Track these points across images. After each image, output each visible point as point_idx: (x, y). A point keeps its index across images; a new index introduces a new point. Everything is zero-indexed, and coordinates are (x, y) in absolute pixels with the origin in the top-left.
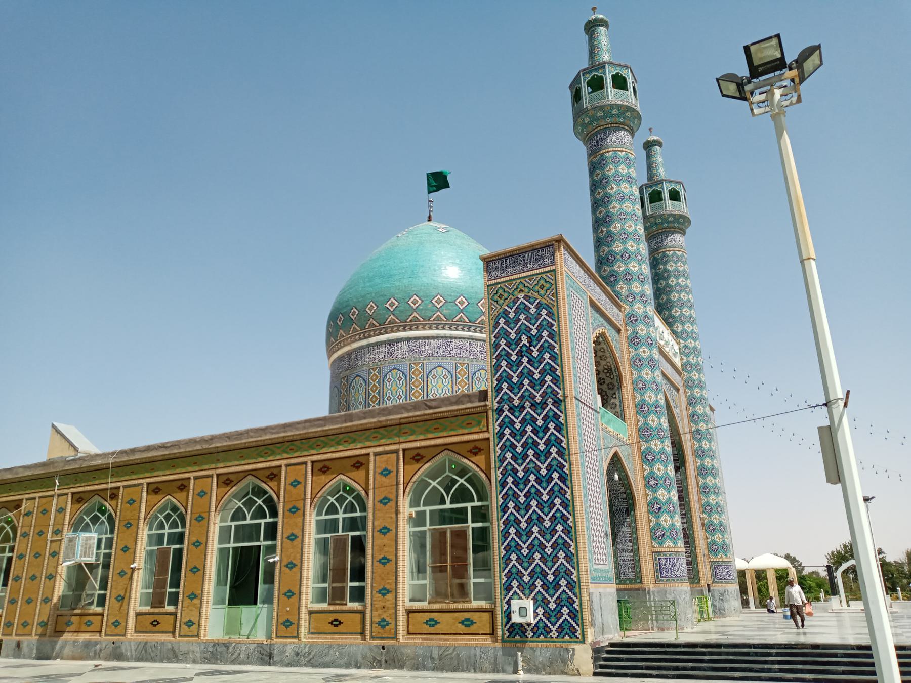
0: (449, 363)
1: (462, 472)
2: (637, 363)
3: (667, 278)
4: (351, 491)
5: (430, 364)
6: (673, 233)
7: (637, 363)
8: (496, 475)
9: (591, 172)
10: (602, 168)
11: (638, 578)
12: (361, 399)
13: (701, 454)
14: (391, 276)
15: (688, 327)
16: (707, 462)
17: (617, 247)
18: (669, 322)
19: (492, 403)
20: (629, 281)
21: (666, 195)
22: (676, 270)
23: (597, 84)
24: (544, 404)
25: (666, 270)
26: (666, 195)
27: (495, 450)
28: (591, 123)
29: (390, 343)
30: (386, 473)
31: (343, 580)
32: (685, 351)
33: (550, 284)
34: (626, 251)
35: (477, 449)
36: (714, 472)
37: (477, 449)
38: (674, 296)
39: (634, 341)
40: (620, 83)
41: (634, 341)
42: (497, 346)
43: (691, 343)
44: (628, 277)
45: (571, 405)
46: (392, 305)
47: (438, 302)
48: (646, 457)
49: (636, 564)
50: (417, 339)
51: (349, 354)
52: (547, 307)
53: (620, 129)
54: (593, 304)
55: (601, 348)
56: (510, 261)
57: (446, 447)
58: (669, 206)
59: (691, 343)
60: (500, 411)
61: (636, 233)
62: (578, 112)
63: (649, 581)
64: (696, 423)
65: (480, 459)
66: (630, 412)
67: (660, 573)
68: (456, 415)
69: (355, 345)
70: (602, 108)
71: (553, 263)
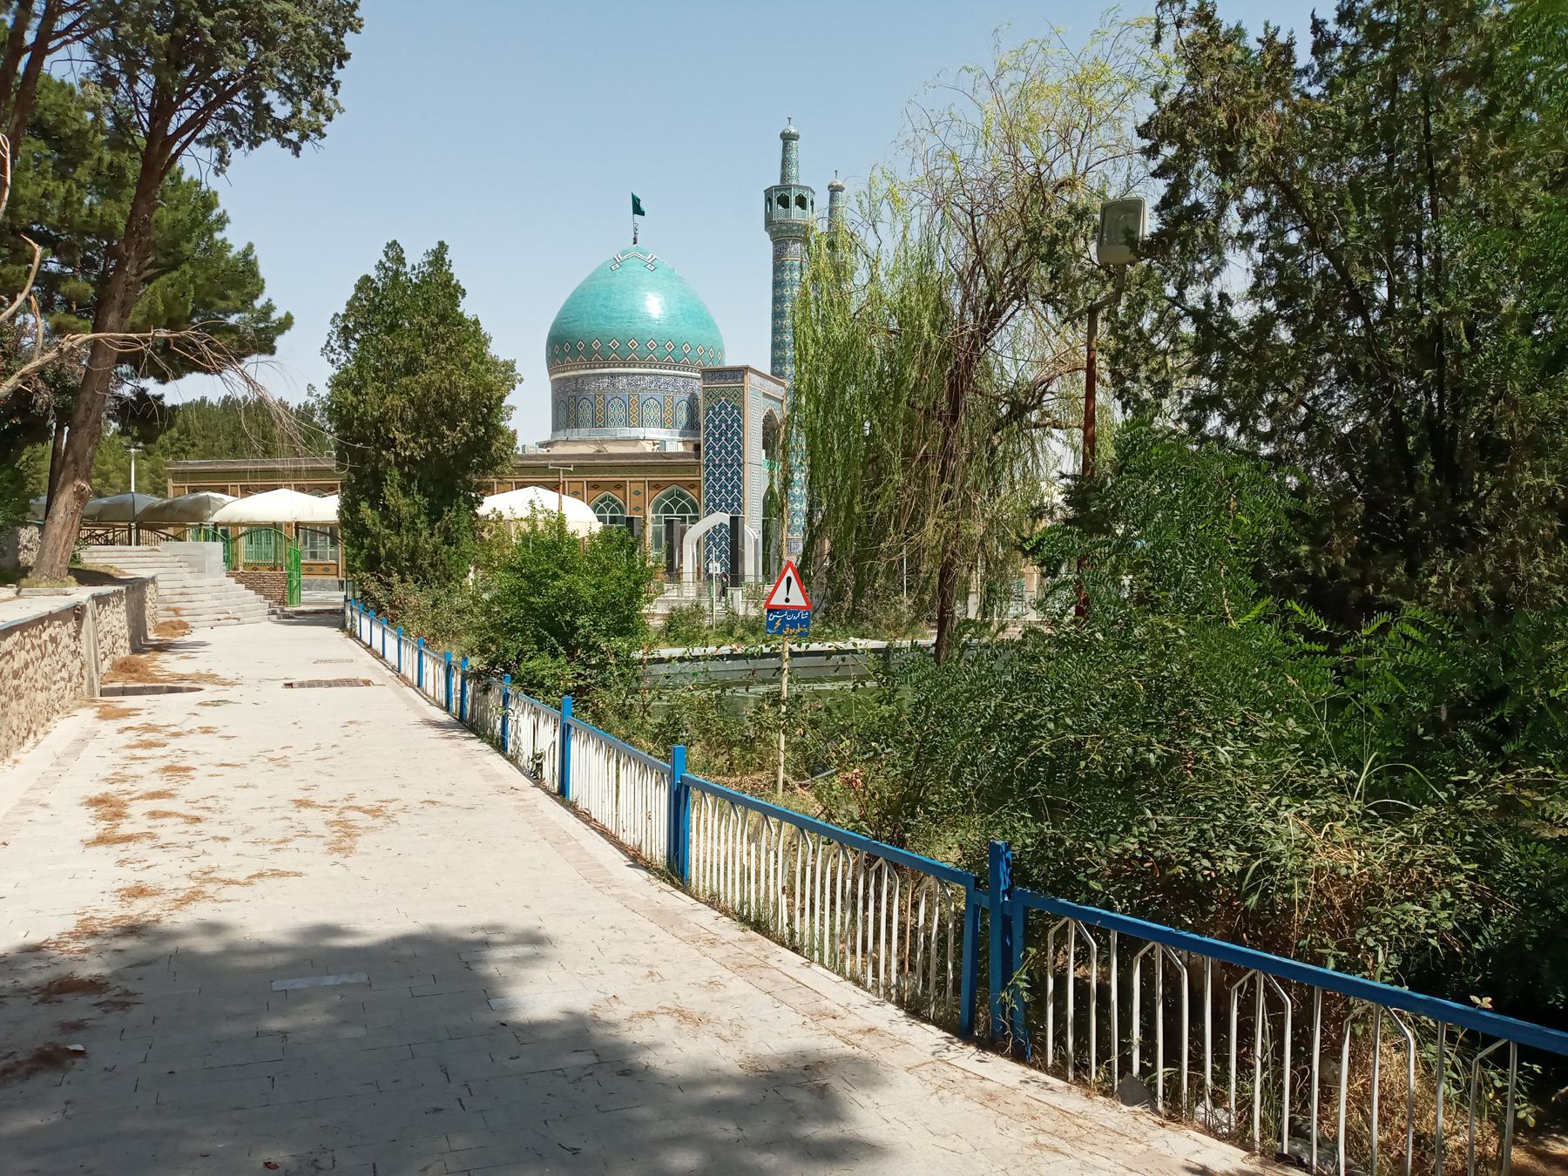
0: (659, 396)
4: (614, 501)
5: (645, 395)
8: (704, 501)
12: (589, 416)
14: (612, 318)
27: (704, 487)
29: (613, 375)
30: (637, 493)
33: (740, 394)
35: (693, 485)
37: (693, 485)
40: (801, 202)
51: (576, 378)
57: (675, 482)
62: (769, 223)
65: (695, 491)
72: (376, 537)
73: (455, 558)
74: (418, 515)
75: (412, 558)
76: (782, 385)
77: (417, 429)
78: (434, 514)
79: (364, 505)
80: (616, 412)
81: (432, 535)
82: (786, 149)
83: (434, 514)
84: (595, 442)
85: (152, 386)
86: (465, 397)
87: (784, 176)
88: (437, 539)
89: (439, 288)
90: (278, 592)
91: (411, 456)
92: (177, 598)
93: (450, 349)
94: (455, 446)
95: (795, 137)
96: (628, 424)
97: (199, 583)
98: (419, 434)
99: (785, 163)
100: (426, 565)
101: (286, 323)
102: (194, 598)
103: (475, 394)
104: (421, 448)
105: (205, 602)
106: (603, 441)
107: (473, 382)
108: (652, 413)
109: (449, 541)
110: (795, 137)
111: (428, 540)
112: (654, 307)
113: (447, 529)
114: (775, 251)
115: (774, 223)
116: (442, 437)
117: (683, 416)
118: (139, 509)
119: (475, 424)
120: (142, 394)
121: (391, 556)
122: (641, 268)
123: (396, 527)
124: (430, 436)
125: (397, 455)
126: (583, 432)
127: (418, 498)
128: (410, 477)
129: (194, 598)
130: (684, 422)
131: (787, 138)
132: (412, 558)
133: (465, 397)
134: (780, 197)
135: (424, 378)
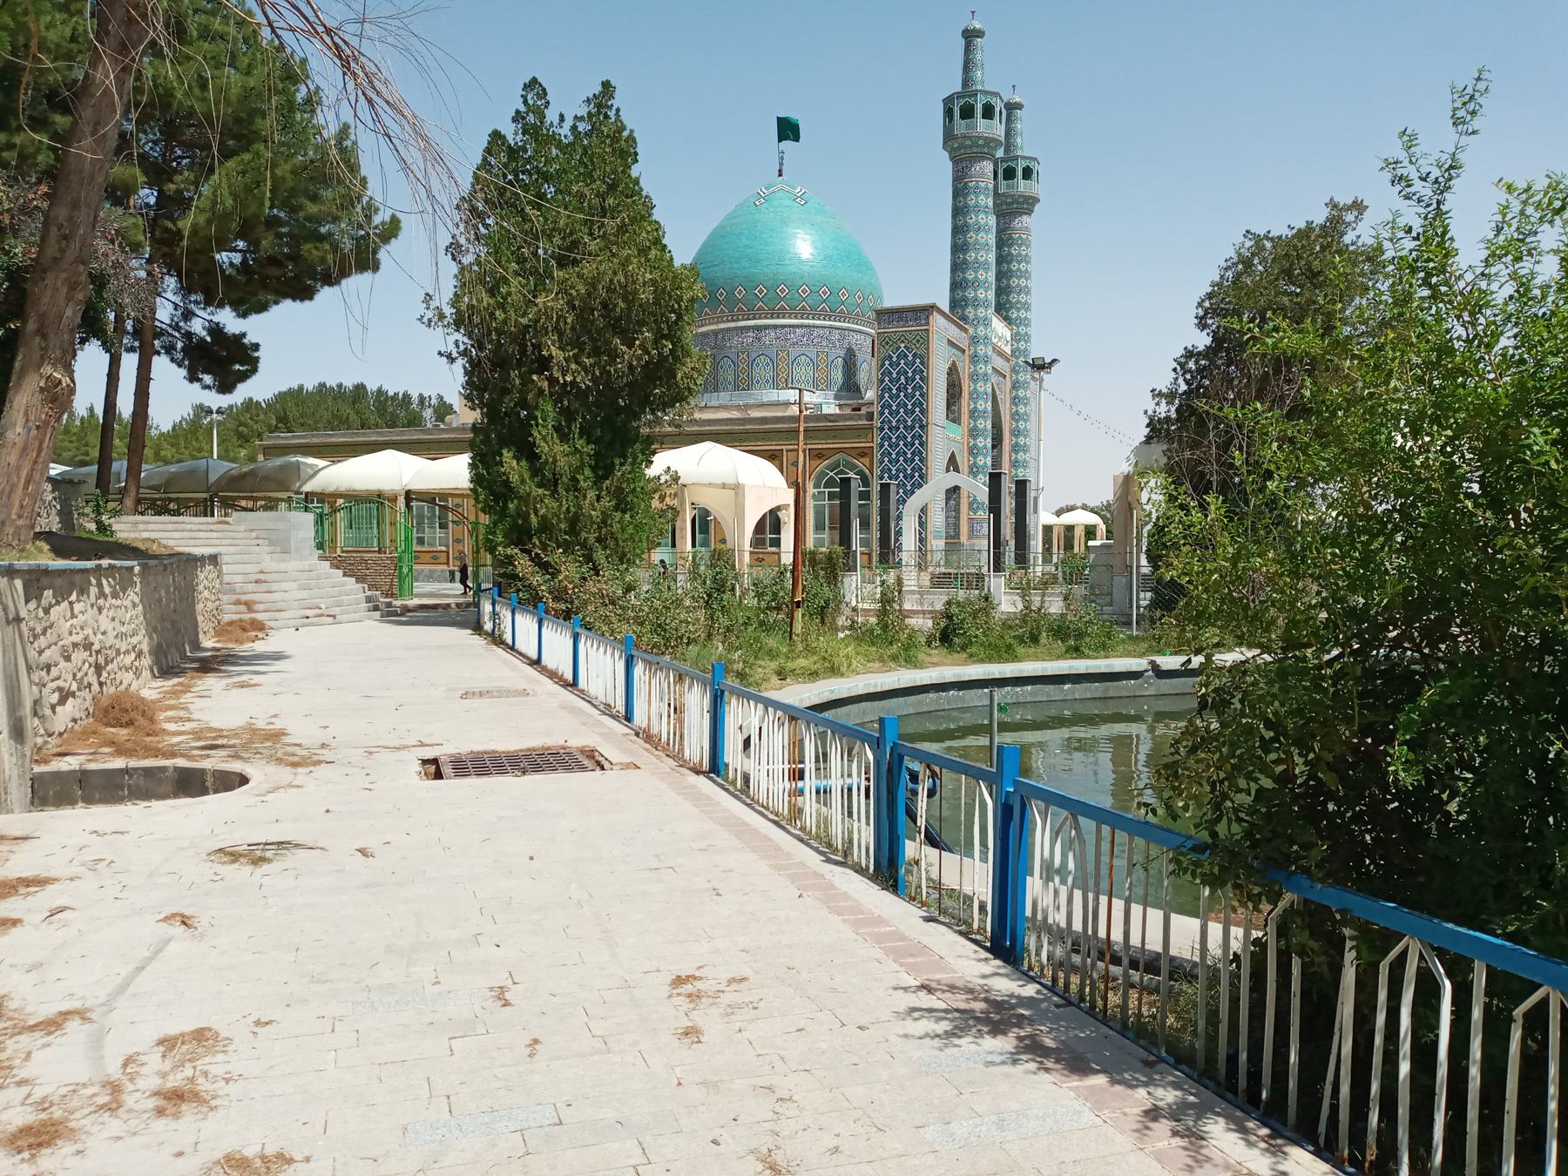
1: (853, 467)
2: (974, 377)
3: (1009, 263)
5: (794, 352)
6: (1021, 214)
7: (974, 377)
8: (877, 472)
9: (954, 216)
10: (965, 196)
11: (957, 535)
12: (730, 378)
13: (1016, 433)
15: (1022, 314)
16: (1021, 440)
17: (970, 275)
18: (1007, 320)
19: (877, 423)
20: (976, 307)
21: (1020, 173)
22: (1019, 255)
23: (968, 113)
24: (913, 427)
25: (1009, 254)
26: (1020, 173)
27: (877, 456)
28: (959, 148)
29: (758, 328)
31: (763, 532)
32: (1016, 337)
33: (924, 339)
34: (976, 280)
35: (863, 453)
36: (1025, 449)
37: (863, 453)
38: (1013, 298)
39: (975, 359)
40: (988, 112)
41: (975, 359)
42: (882, 381)
43: (1022, 329)
44: (976, 303)
45: (932, 430)
46: (761, 291)
47: (804, 291)
48: (973, 451)
49: (957, 526)
50: (783, 326)
51: (715, 333)
52: (921, 357)
53: (984, 159)
54: (950, 343)
55: (953, 371)
56: (896, 316)
57: (841, 450)
58: (1022, 186)
59: (1022, 329)
60: (882, 429)
61: (986, 262)
62: (949, 136)
63: (964, 538)
64: (1016, 405)
65: (866, 460)
66: (965, 417)
67: (972, 533)
68: (850, 428)
69: (722, 326)
70: (970, 138)
71: (927, 324)
72: (525, 499)
73: (630, 530)
74: (580, 469)
75: (573, 529)
76: (966, 331)
77: (580, 346)
78: (602, 470)
79: (507, 455)
80: (762, 371)
81: (599, 498)
82: (968, 49)
83: (602, 470)
84: (738, 407)
85: (228, 319)
86: (646, 295)
87: (966, 82)
88: (607, 503)
89: (605, 148)
90: (384, 581)
91: (574, 383)
92: (251, 587)
93: (622, 229)
94: (631, 367)
95: (979, 34)
96: (776, 386)
97: (283, 566)
98: (582, 351)
99: (968, 66)
100: (592, 538)
101: (391, 230)
102: (274, 587)
103: (659, 292)
104: (585, 369)
105: (289, 592)
106: (747, 407)
107: (656, 275)
108: (803, 373)
109: (622, 505)
110: (979, 34)
111: (594, 505)
112: (804, 247)
113: (619, 490)
114: (955, 171)
115: (955, 138)
116: (614, 355)
117: (838, 376)
118: (213, 478)
119: (659, 337)
120: (216, 330)
121: (546, 527)
122: (790, 203)
123: (552, 484)
124: (596, 352)
125: (552, 381)
126: (724, 397)
127: (580, 443)
128: (568, 414)
129: (274, 587)
130: (840, 381)
131: (970, 35)
132: (573, 529)
133: (646, 295)
134: (962, 108)
135: (588, 269)
